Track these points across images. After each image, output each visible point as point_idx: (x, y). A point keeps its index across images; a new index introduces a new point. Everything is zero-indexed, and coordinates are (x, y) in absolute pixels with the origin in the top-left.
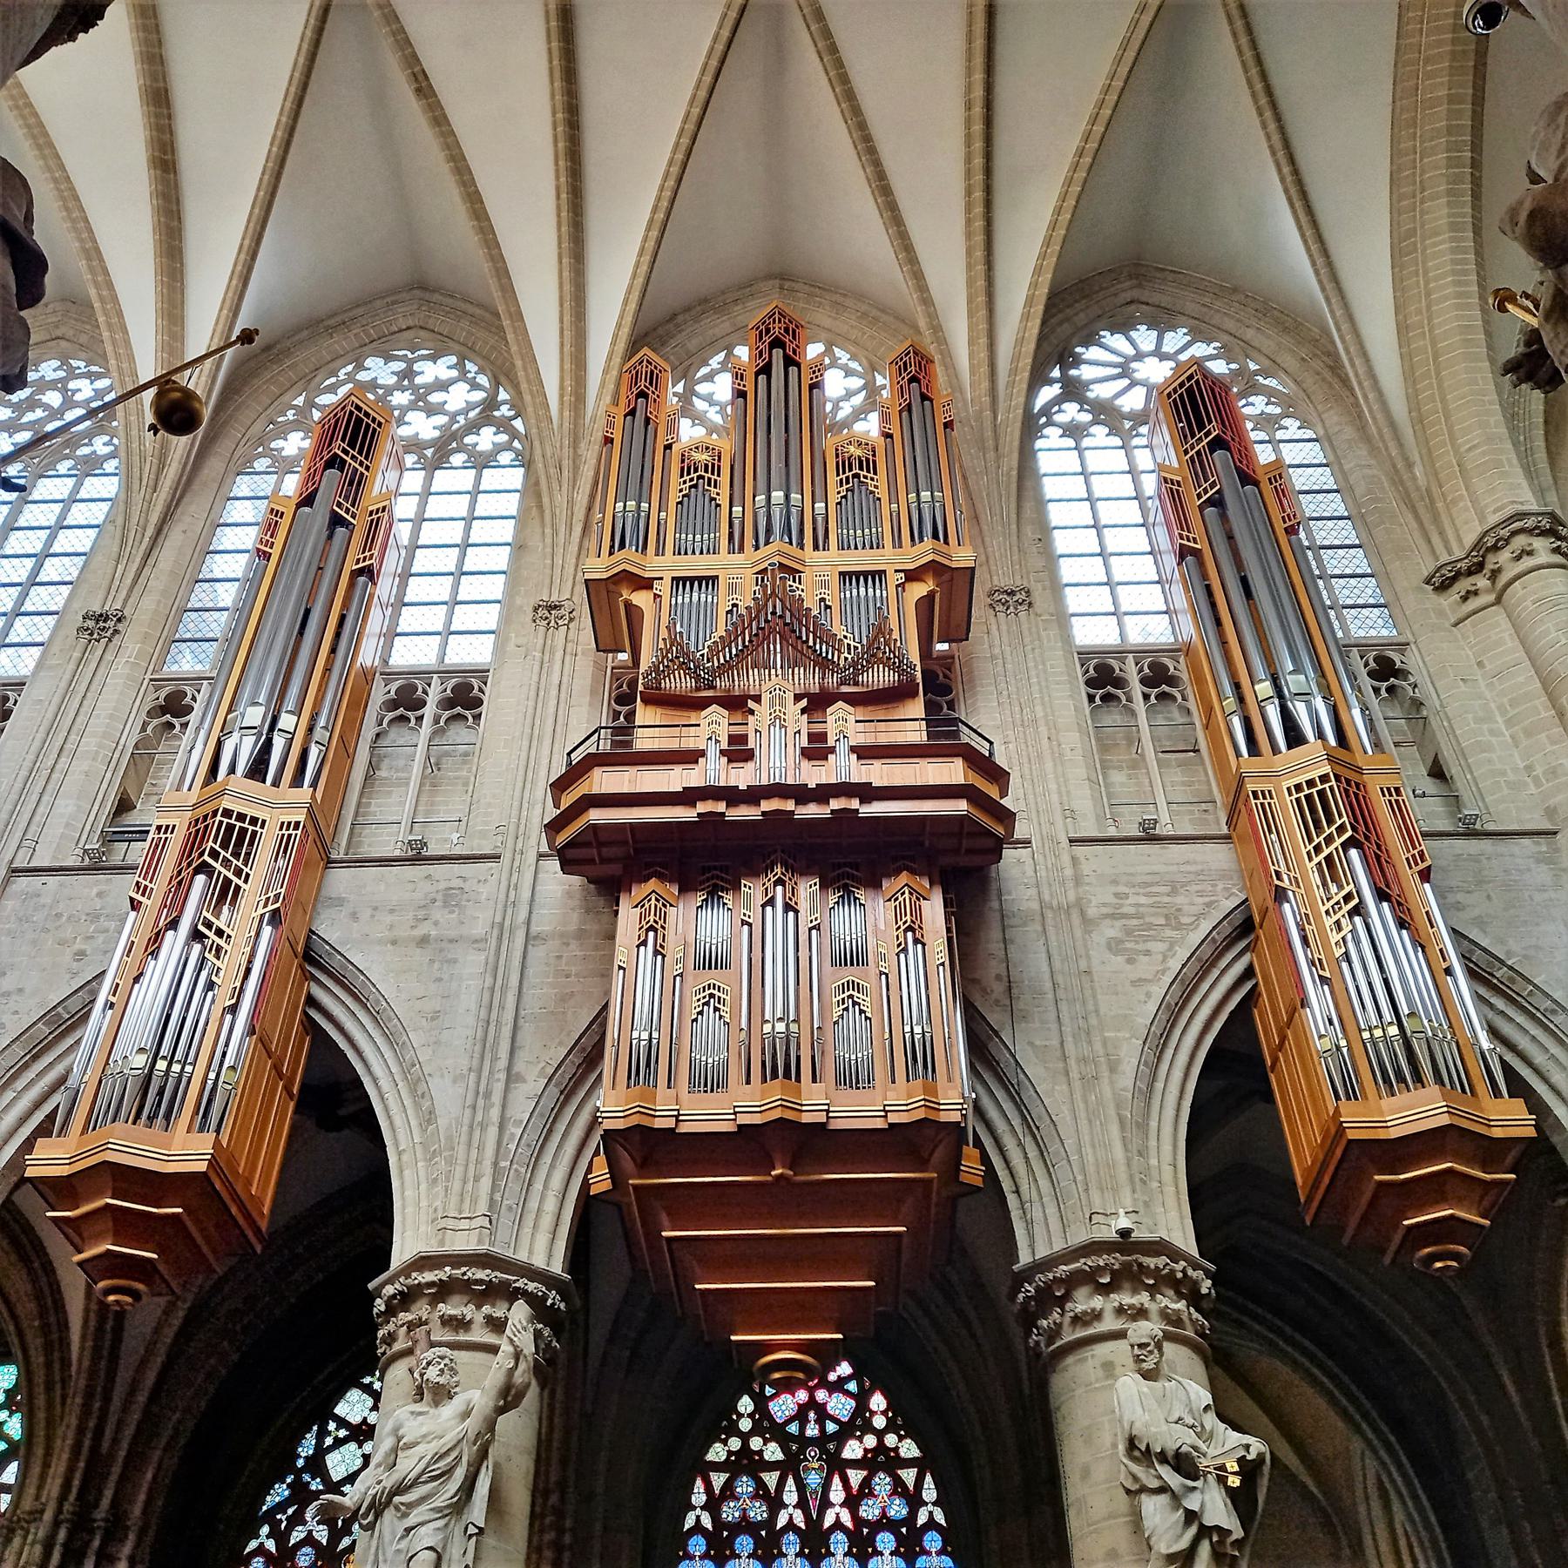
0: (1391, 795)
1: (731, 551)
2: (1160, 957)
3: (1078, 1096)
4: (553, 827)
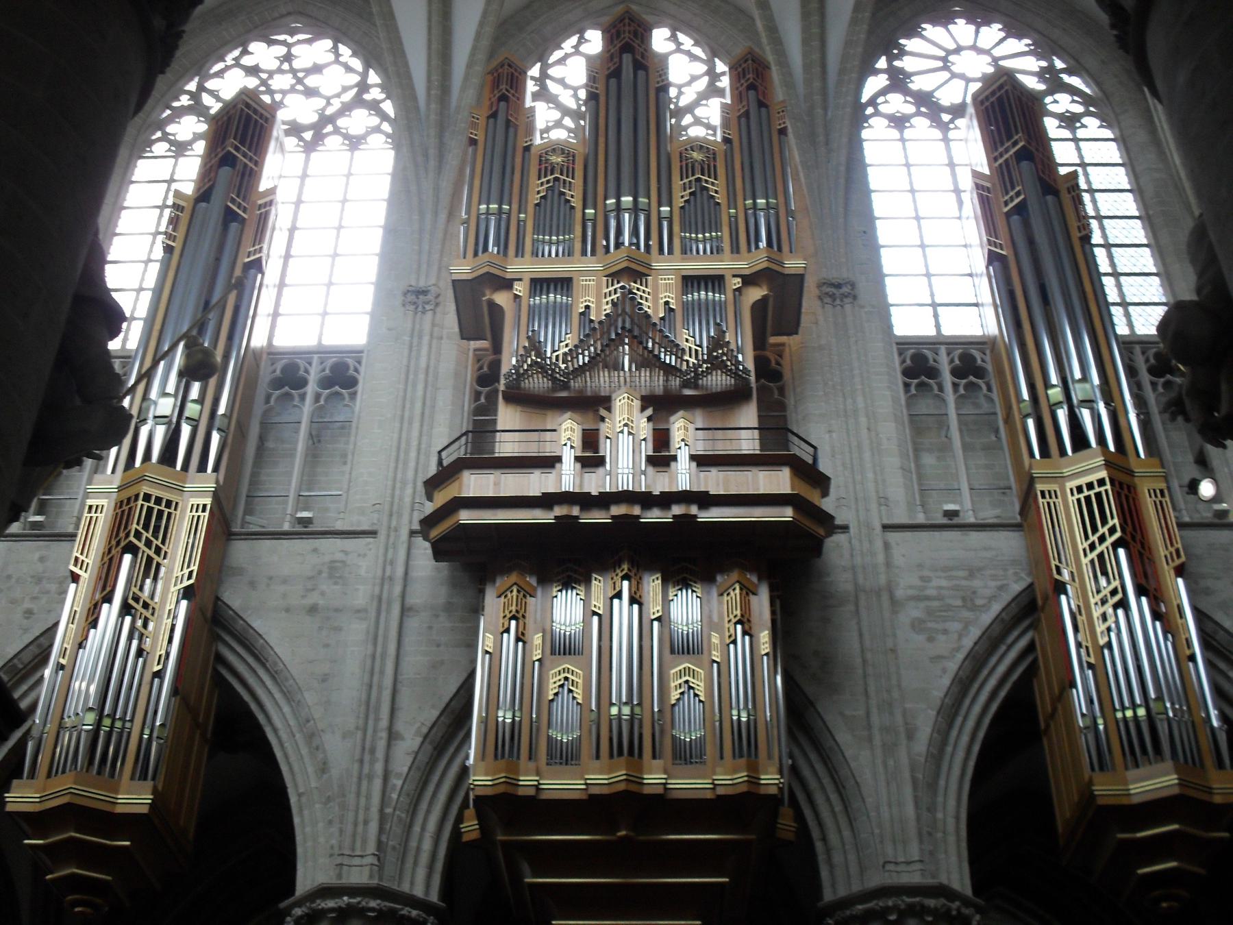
0: (1156, 496)
1: (584, 253)
2: (956, 636)
3: (879, 761)
4: (429, 522)
